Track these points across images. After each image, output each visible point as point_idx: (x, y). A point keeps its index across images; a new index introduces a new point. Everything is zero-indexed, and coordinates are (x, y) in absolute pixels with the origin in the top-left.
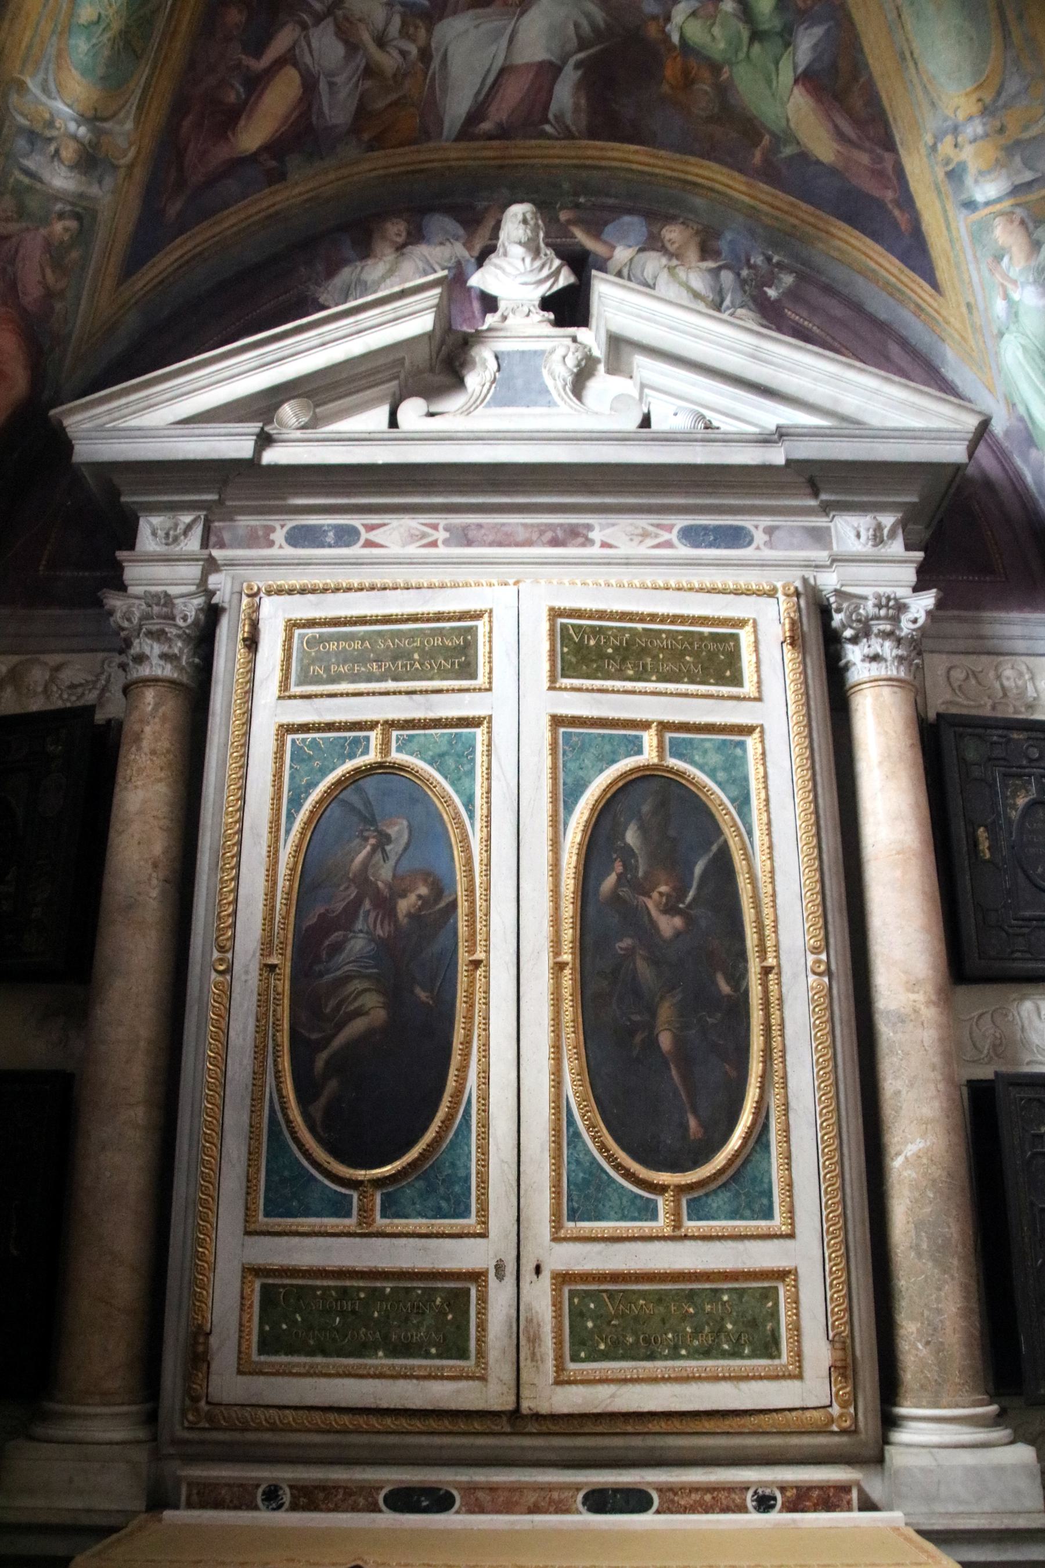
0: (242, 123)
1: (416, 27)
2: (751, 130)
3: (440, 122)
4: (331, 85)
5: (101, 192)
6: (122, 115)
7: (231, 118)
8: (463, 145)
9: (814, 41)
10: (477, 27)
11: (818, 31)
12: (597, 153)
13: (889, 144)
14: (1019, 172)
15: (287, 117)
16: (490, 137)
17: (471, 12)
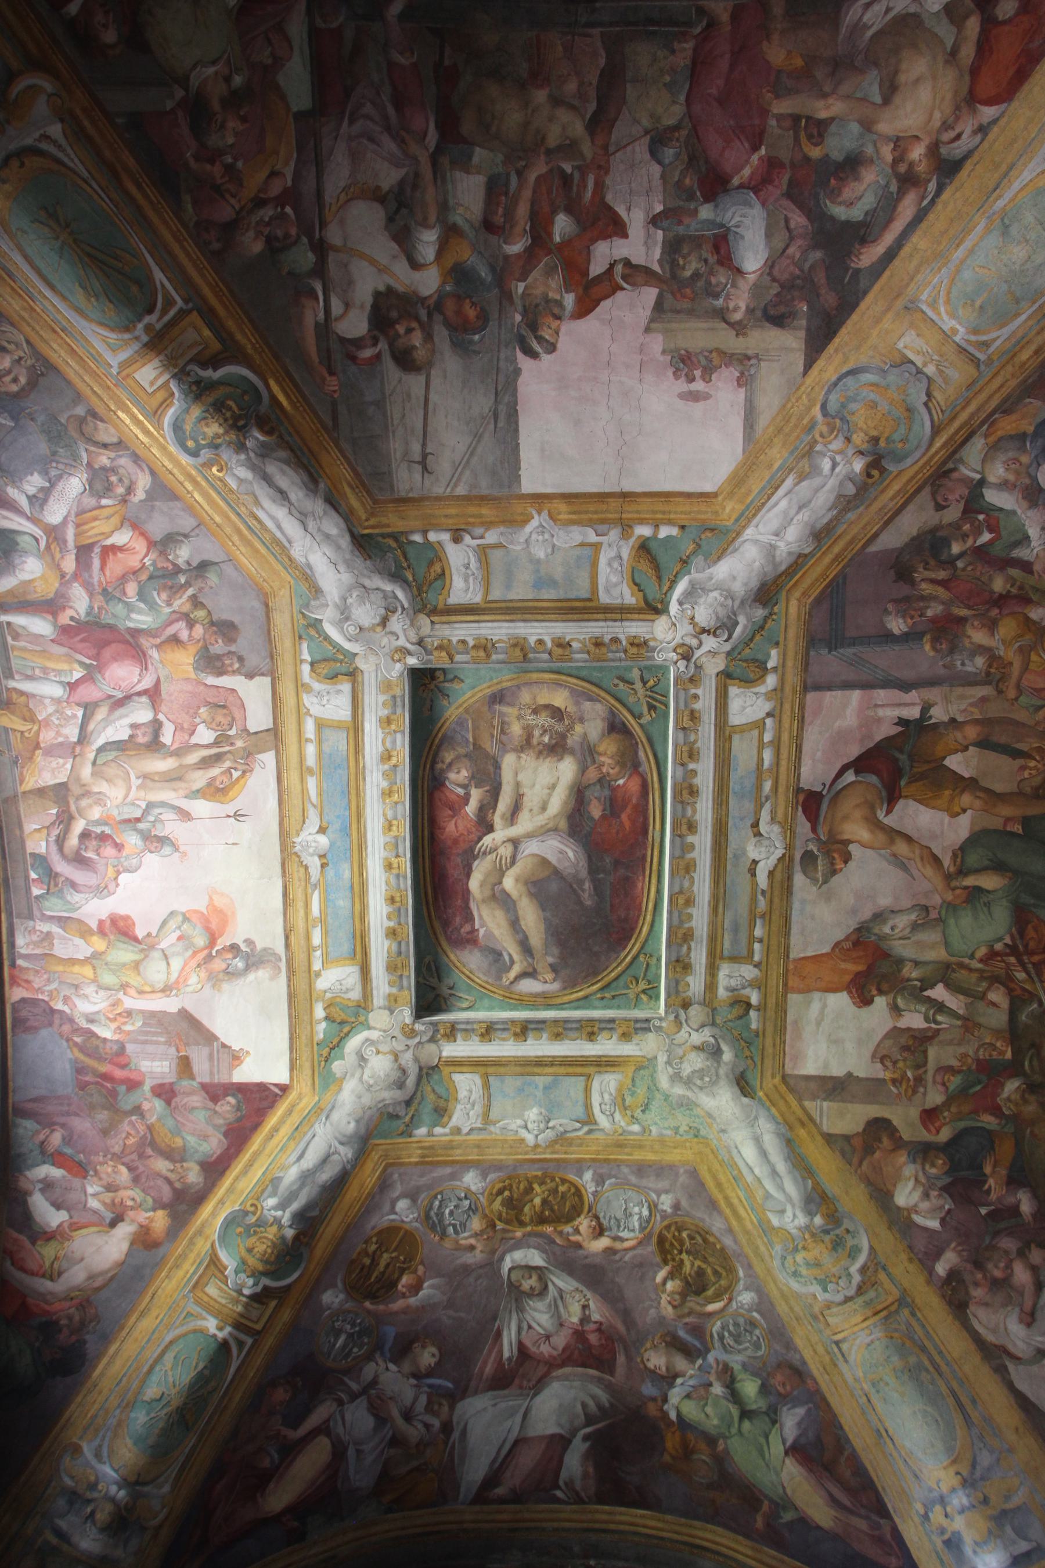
0: (272, 1485)
1: (440, 1404)
2: (749, 1496)
4: (358, 1451)
8: (477, 1508)
9: (797, 1419)
10: (495, 1405)
11: (801, 1411)
12: (605, 1517)
16: (502, 1501)
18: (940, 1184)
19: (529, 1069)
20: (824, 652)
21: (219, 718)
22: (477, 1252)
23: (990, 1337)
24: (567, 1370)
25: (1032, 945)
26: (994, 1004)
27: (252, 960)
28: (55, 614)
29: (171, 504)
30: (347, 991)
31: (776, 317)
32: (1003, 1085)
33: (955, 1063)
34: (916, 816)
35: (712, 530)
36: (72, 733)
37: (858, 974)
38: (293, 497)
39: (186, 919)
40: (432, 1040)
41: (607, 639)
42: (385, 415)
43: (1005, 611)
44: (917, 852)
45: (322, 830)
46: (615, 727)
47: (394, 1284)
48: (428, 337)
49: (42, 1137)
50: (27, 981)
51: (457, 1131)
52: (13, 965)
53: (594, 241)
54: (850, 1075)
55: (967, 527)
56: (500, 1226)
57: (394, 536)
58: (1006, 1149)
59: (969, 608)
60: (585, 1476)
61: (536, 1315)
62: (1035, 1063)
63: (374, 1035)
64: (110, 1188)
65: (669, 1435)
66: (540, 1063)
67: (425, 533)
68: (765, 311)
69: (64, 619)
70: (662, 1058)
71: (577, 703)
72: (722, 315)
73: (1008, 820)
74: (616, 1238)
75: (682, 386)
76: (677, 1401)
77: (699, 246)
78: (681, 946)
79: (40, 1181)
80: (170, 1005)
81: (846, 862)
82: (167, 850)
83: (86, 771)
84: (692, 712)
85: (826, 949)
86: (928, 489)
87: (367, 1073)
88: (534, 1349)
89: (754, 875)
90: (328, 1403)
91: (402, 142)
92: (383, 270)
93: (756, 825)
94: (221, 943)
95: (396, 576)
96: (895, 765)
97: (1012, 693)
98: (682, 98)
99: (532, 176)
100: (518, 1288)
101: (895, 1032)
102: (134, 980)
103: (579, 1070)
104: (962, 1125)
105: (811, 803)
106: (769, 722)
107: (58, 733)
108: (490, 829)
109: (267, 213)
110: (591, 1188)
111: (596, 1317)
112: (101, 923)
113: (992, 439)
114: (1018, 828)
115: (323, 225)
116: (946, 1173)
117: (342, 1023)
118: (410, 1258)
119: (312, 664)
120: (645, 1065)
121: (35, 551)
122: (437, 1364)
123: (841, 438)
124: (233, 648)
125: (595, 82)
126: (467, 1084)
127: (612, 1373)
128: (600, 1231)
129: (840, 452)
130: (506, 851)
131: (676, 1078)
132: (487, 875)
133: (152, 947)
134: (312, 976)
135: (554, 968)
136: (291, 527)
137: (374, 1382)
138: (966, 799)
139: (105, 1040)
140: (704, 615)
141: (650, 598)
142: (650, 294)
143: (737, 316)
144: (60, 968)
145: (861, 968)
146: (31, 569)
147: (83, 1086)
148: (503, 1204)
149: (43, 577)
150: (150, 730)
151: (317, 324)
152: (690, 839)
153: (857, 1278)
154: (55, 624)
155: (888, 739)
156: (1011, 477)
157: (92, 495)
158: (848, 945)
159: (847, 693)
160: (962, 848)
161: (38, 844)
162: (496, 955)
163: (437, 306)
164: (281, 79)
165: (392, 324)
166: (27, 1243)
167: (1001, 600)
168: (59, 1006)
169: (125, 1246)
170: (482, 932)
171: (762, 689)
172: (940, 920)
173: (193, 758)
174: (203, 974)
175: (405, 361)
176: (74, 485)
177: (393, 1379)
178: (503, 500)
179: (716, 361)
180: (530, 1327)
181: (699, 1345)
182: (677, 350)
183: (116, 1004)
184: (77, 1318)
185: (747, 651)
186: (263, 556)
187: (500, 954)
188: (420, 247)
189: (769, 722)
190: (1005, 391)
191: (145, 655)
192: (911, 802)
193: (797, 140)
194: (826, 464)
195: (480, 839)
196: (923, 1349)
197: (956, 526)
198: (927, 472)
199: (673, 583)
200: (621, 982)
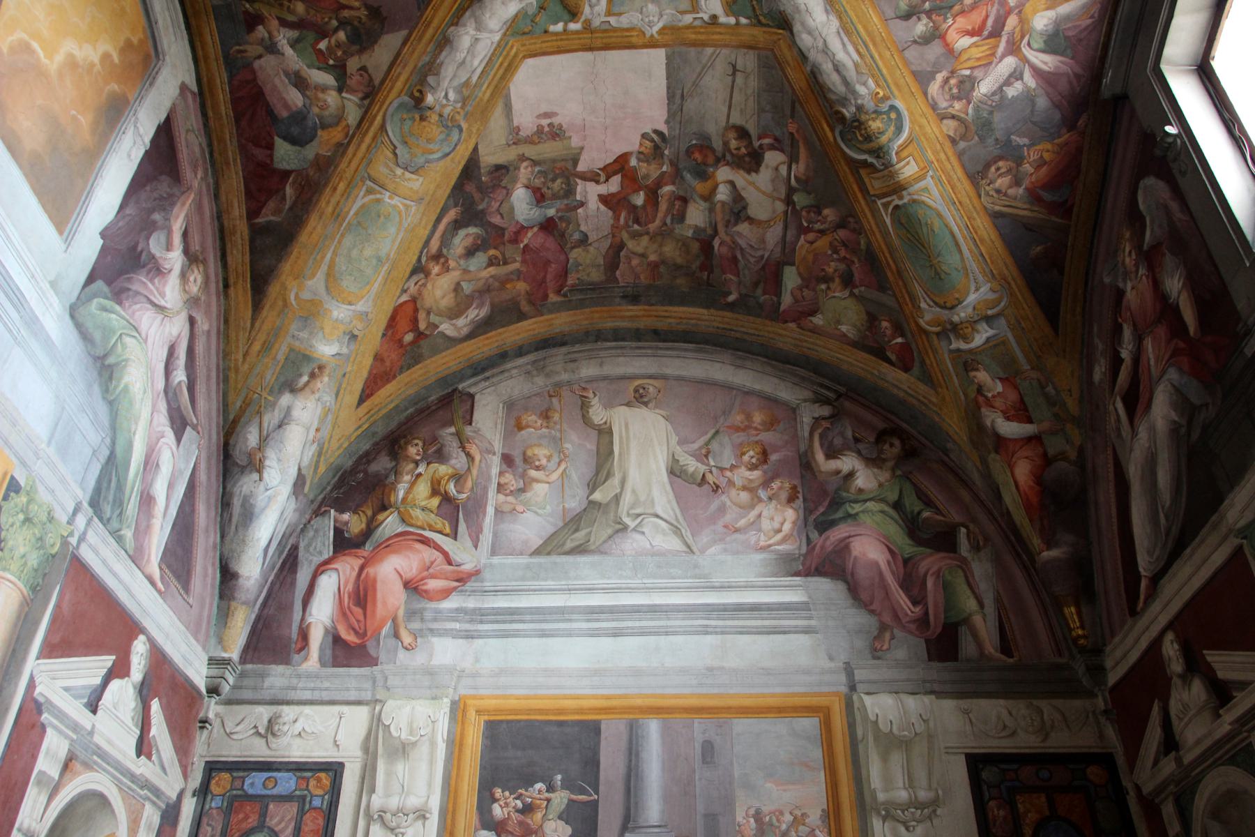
29: (919, 69)
31: (501, 170)
35: (524, 33)
38: (830, 66)
42: (759, 103)
48: (726, 144)
53: (618, 193)
55: (339, 53)
67: (738, 24)
68: (508, 170)
72: (535, 163)
77: (553, 195)
86: (377, 82)
92: (752, 183)
99: (658, 222)
109: (817, 226)
113: (343, 124)
115: (786, 213)
121: (1034, 34)
123: (445, 115)
129: (444, 106)
136: (835, 45)
142: (581, 167)
143: (525, 164)
149: (1035, 12)
151: (797, 163)
156: (321, 95)
157: (975, 78)
163: (718, 161)
164: (799, 281)
165: (749, 154)
175: (742, 133)
176: (985, 87)
178: (680, 44)
179: (535, 138)
186: (860, 22)
193: (503, 255)
197: (348, 54)
198: (380, 97)
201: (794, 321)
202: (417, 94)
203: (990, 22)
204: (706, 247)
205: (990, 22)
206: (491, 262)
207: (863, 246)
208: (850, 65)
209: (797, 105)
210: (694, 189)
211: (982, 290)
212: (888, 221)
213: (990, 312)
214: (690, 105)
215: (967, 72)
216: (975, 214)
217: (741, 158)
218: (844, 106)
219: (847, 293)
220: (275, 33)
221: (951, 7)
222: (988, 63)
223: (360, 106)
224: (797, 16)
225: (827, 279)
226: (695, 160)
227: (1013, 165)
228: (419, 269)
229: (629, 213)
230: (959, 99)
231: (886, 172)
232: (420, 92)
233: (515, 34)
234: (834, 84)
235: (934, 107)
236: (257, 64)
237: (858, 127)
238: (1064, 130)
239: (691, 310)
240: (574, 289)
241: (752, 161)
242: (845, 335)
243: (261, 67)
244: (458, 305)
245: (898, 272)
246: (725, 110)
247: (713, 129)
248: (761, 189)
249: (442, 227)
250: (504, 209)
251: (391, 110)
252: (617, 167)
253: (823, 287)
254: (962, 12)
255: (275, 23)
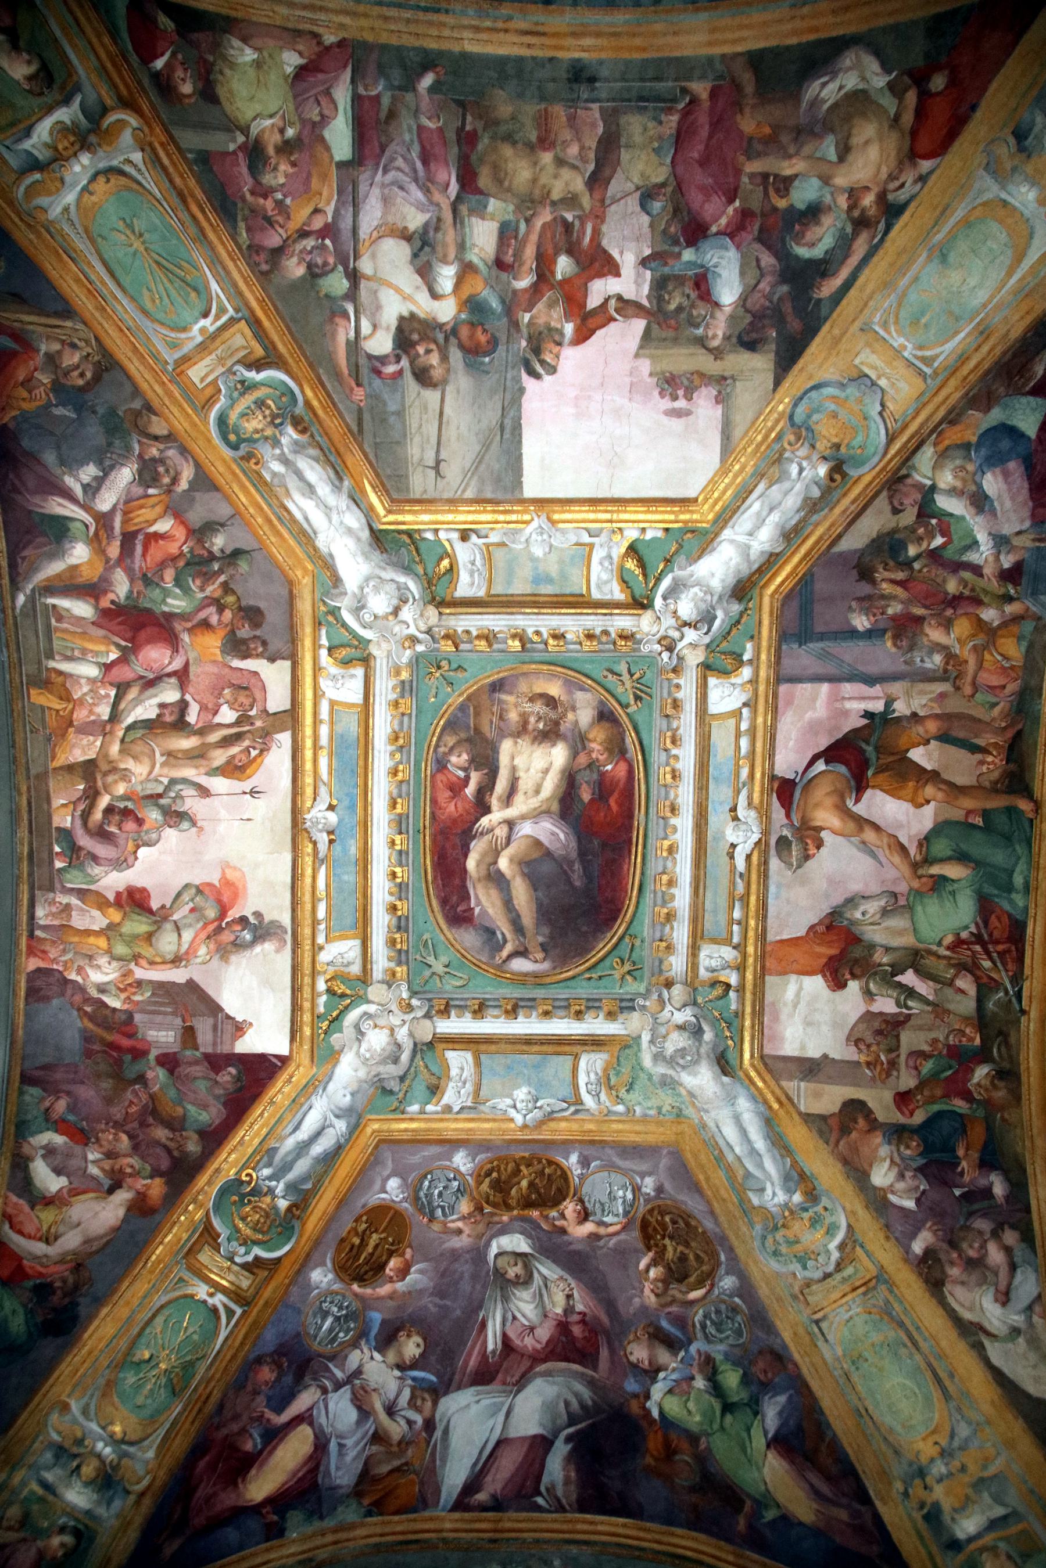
0: (253, 1472)
3: (438, 1491)
5: (109, 1514)
6: (146, 1443)
7: (245, 1464)
8: (457, 1515)
9: (778, 1408)
11: (782, 1399)
12: (585, 1527)
13: (864, 1498)
14: (990, 1508)
15: (294, 1474)
16: (483, 1508)
17: (473, 1389)
18: (915, 1165)
19: (519, 1047)
20: (795, 646)
21: (242, 699)
22: (464, 1236)
23: (967, 1315)
24: (549, 1365)
25: (996, 934)
26: (962, 991)
27: (260, 932)
28: (97, 599)
30: (349, 964)
31: (749, 343)
32: (973, 1071)
33: (926, 1048)
34: (883, 806)
36: (104, 711)
37: (831, 958)
38: (320, 491)
39: (199, 891)
40: (428, 1016)
41: (598, 631)
42: (404, 423)
43: (960, 611)
44: (885, 840)
45: (331, 808)
46: (605, 716)
47: (382, 1267)
48: (444, 358)
49: (47, 1104)
50: (44, 952)
51: (448, 1109)
52: (31, 935)
53: (592, 278)
54: (825, 1056)
55: (921, 531)
56: (488, 1210)
57: (409, 534)
58: (978, 1133)
59: (926, 607)
60: (567, 1482)
61: (521, 1305)
62: (1003, 1049)
63: (372, 1008)
64: (110, 1155)
65: (651, 1436)
66: (528, 1041)
68: (739, 337)
69: (105, 603)
70: (646, 1037)
71: (570, 693)
72: (701, 342)
73: (969, 812)
74: (600, 1223)
75: (666, 404)
76: (659, 1397)
77: (683, 284)
78: (663, 925)
79: (43, 1147)
80: (178, 976)
81: (818, 848)
82: (185, 825)
83: (115, 748)
84: (675, 701)
85: (802, 933)
86: (885, 493)
87: (364, 1046)
88: (518, 1342)
89: (731, 856)
90: (312, 1389)
91: (427, 191)
93: (734, 809)
94: (233, 914)
95: (407, 570)
96: (861, 756)
97: (968, 690)
98: (668, 161)
99: (538, 223)
100: (503, 1275)
101: (868, 1016)
102: (147, 952)
103: (567, 1048)
104: (936, 1108)
105: (785, 790)
106: (745, 711)
107: (91, 712)
108: (487, 810)
109: (310, 243)
110: (577, 1171)
111: (580, 1307)
112: (118, 895)
113: (941, 447)
114: (978, 821)
116: (921, 1154)
117: (343, 996)
118: (399, 1241)
119: (330, 649)
120: (627, 1045)
122: (422, 1355)
124: (258, 633)
125: (594, 146)
126: (458, 1061)
127: (595, 1368)
128: (584, 1216)
130: (501, 832)
131: (658, 1057)
132: (484, 855)
133: (165, 919)
134: (316, 949)
135: (544, 947)
137: (358, 1372)
138: (929, 790)
139: (114, 1010)
140: (686, 608)
141: (637, 594)
142: (639, 325)
143: (716, 343)
144: (76, 939)
145: (833, 951)
146: (79, 553)
147: (88, 1054)
148: (491, 1187)
149: (90, 562)
150: (176, 710)
151: (348, 341)
152: (673, 821)
153: (835, 1255)
154: (96, 607)
155: (855, 731)
156: (959, 484)
158: (821, 929)
159: (816, 685)
160: (927, 838)
161: (64, 819)
162: (490, 932)
164: (327, 134)
165: (413, 344)
166: (27, 1208)
167: (955, 601)
168: (73, 976)
169: (121, 1212)
170: (477, 910)
171: (738, 681)
172: (910, 908)
173: (214, 737)
174: (212, 946)
175: (423, 376)
176: (125, 475)
177: (378, 1370)
179: (697, 382)
180: (514, 1318)
181: (679, 1334)
182: (663, 373)
183: (130, 972)
184: (71, 1280)
185: (724, 644)
187: (494, 933)
188: (440, 280)
189: (745, 711)
190: (952, 401)
191: (176, 637)
192: (878, 793)
194: (794, 469)
195: (478, 820)
196: (901, 1324)
199: (658, 580)
200: (607, 962)
201: (328, 49)
202: (837, 477)
203: (139, 549)
204: (468, 180)
205: (139, 549)
206: (785, 184)
207: (242, 225)
208: (297, 496)
209: (355, 429)
210: (486, 282)
211: (59, 210)
212: (214, 286)
213: (37, 176)
214: (491, 415)
215: (151, 491)
216: (97, 314)
217: (424, 338)
218: (296, 443)
219: (254, 131)
220: (991, 559)
221: (188, 564)
222: (129, 504)
223: (914, 467)
224: (367, 548)
225: (286, 148)
226: (485, 331)
227: (63, 381)
228: (892, 211)
229: (579, 241)
230: (154, 460)
231: (229, 363)
232: (832, 480)
233: (704, 532)
234: (312, 468)
235: (184, 451)
236: (1027, 524)
237: (274, 417)
238: (12, 426)
239: (490, 50)
240: (667, 102)
241: (410, 333)
242: (245, 40)
243: (1022, 521)
244: (848, 119)
245: (184, 201)
246: (448, 410)
247: (461, 382)
248: (397, 291)
249: (844, 273)
250: (753, 274)
251: (876, 459)
252: (591, 323)
253: (290, 132)
254: (174, 559)
255: (987, 571)
